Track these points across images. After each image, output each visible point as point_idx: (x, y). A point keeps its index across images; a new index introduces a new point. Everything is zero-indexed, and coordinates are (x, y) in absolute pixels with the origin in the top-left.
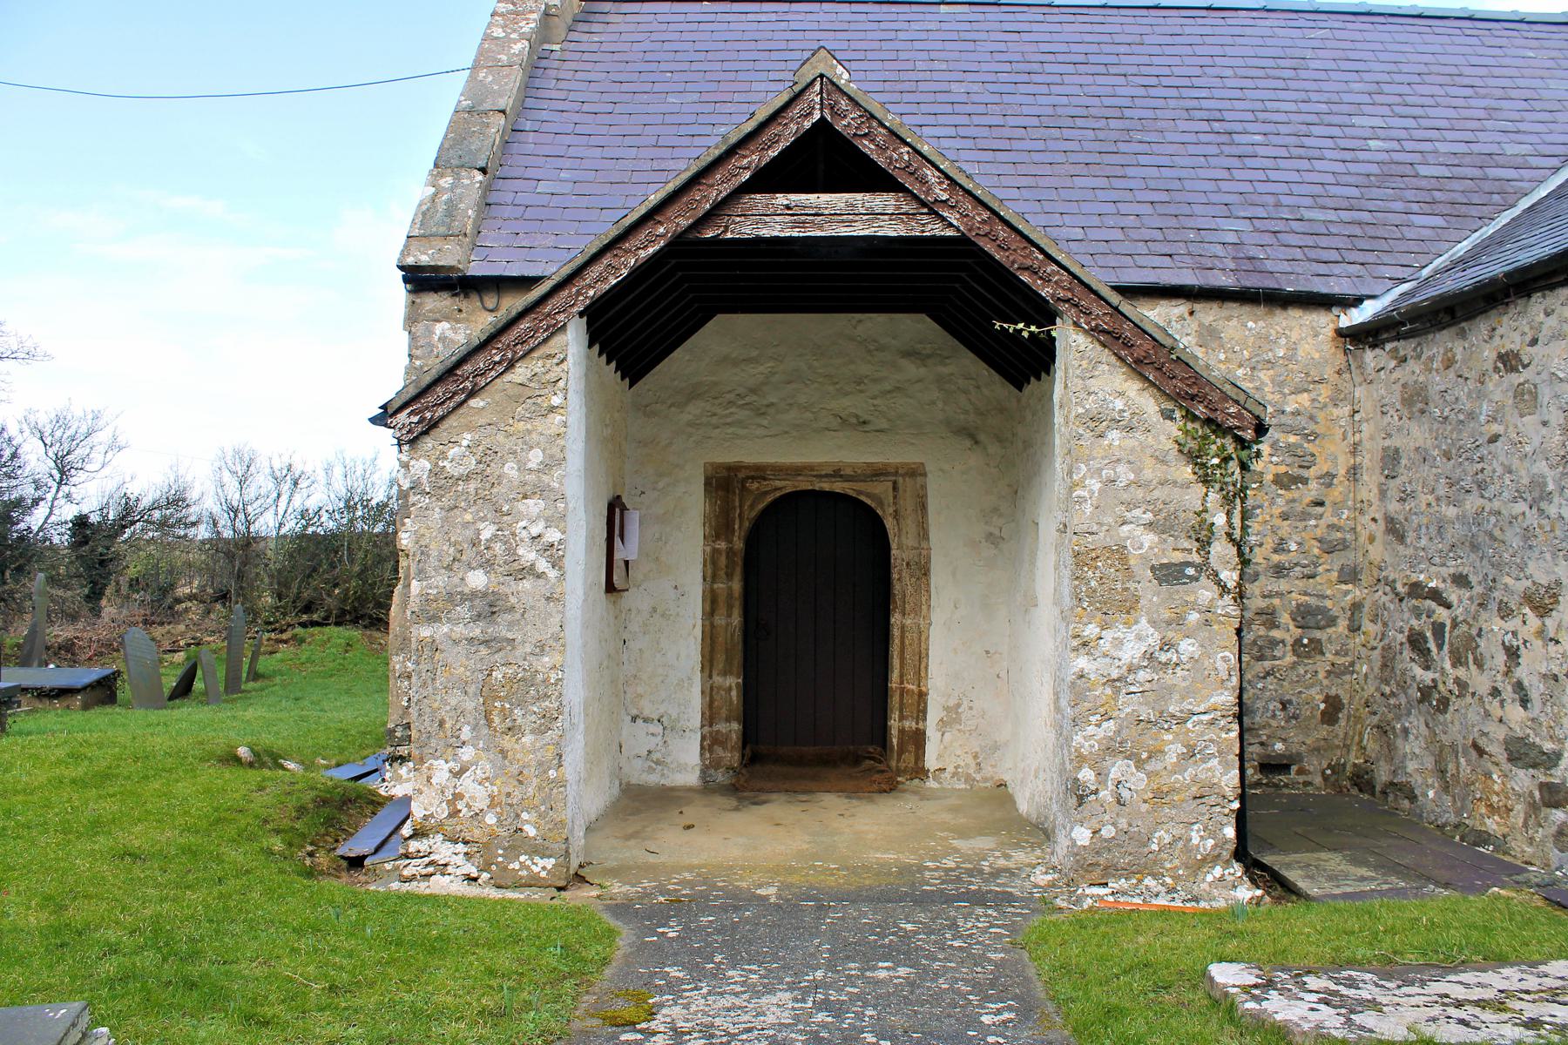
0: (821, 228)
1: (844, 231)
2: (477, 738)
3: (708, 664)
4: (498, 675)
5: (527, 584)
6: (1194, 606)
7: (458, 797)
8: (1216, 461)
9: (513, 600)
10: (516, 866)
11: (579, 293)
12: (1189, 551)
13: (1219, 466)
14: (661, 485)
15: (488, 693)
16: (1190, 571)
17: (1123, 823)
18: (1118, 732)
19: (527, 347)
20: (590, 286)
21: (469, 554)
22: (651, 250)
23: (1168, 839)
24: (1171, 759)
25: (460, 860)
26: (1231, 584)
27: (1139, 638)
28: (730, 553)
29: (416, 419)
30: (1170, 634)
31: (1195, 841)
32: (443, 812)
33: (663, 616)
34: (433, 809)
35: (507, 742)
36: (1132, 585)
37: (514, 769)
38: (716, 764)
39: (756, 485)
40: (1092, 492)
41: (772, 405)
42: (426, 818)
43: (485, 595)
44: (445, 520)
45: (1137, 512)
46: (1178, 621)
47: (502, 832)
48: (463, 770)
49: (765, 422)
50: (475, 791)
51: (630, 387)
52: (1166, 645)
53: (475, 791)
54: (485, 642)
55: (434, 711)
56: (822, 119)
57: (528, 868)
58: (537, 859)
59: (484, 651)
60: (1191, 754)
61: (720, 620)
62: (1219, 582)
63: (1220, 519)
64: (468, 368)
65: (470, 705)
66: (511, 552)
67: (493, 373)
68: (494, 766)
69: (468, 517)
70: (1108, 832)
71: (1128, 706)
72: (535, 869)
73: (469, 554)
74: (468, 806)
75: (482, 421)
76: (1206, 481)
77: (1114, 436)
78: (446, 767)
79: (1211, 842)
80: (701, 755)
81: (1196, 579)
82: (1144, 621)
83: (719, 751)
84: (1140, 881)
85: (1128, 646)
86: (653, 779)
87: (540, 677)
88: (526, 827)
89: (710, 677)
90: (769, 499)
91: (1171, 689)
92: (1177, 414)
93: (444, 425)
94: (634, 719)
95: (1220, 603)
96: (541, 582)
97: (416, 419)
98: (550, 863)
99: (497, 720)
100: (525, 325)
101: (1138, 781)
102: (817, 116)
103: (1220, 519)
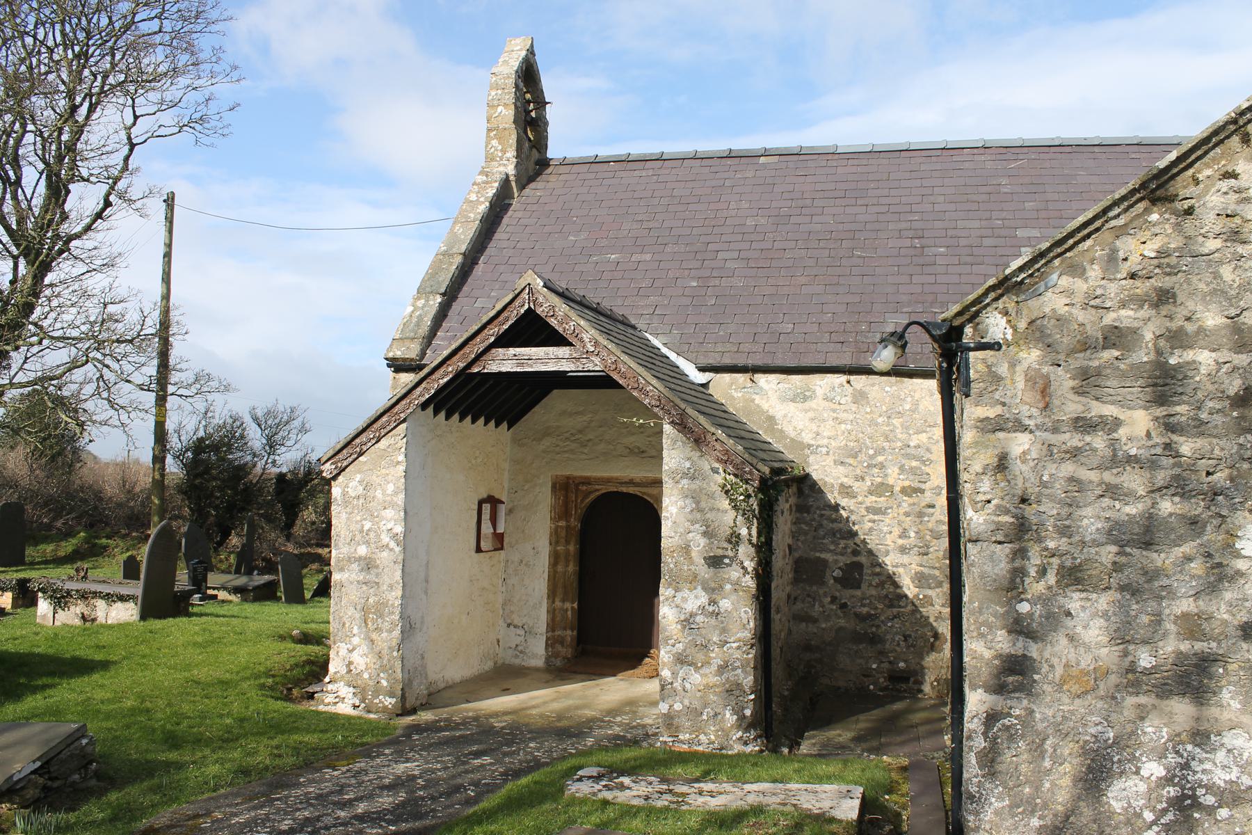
0: (532, 366)
2: (360, 633)
3: (552, 594)
4: (371, 600)
5: (385, 554)
6: (729, 581)
7: (350, 663)
8: (742, 497)
9: (378, 562)
10: (376, 701)
11: (410, 403)
12: (727, 549)
13: (744, 500)
14: (526, 488)
15: (365, 610)
16: (727, 561)
17: (686, 702)
19: (386, 431)
20: (415, 399)
21: (358, 537)
22: (445, 380)
26: (750, 569)
28: (568, 528)
29: (333, 467)
30: (714, 596)
32: (344, 670)
33: (526, 565)
34: (339, 669)
36: (693, 568)
38: (556, 655)
39: (585, 488)
40: (672, 514)
41: (589, 440)
42: (335, 673)
43: (365, 558)
44: (348, 519)
45: (697, 526)
47: (371, 683)
48: (354, 649)
49: (586, 451)
51: (509, 429)
55: (341, 618)
56: (530, 308)
59: (365, 588)
61: (560, 568)
62: (743, 568)
63: (744, 532)
64: (358, 441)
66: (378, 536)
67: (370, 444)
72: (386, 703)
73: (358, 537)
75: (366, 468)
76: (735, 508)
80: (546, 648)
81: (728, 565)
82: (699, 587)
83: (559, 647)
84: (697, 736)
85: (690, 602)
86: (517, 662)
88: (383, 681)
89: (553, 602)
90: (593, 497)
92: (721, 471)
93: (347, 470)
94: (509, 625)
95: (744, 579)
97: (333, 467)
98: (393, 701)
100: (384, 419)
102: (526, 307)
103: (744, 532)
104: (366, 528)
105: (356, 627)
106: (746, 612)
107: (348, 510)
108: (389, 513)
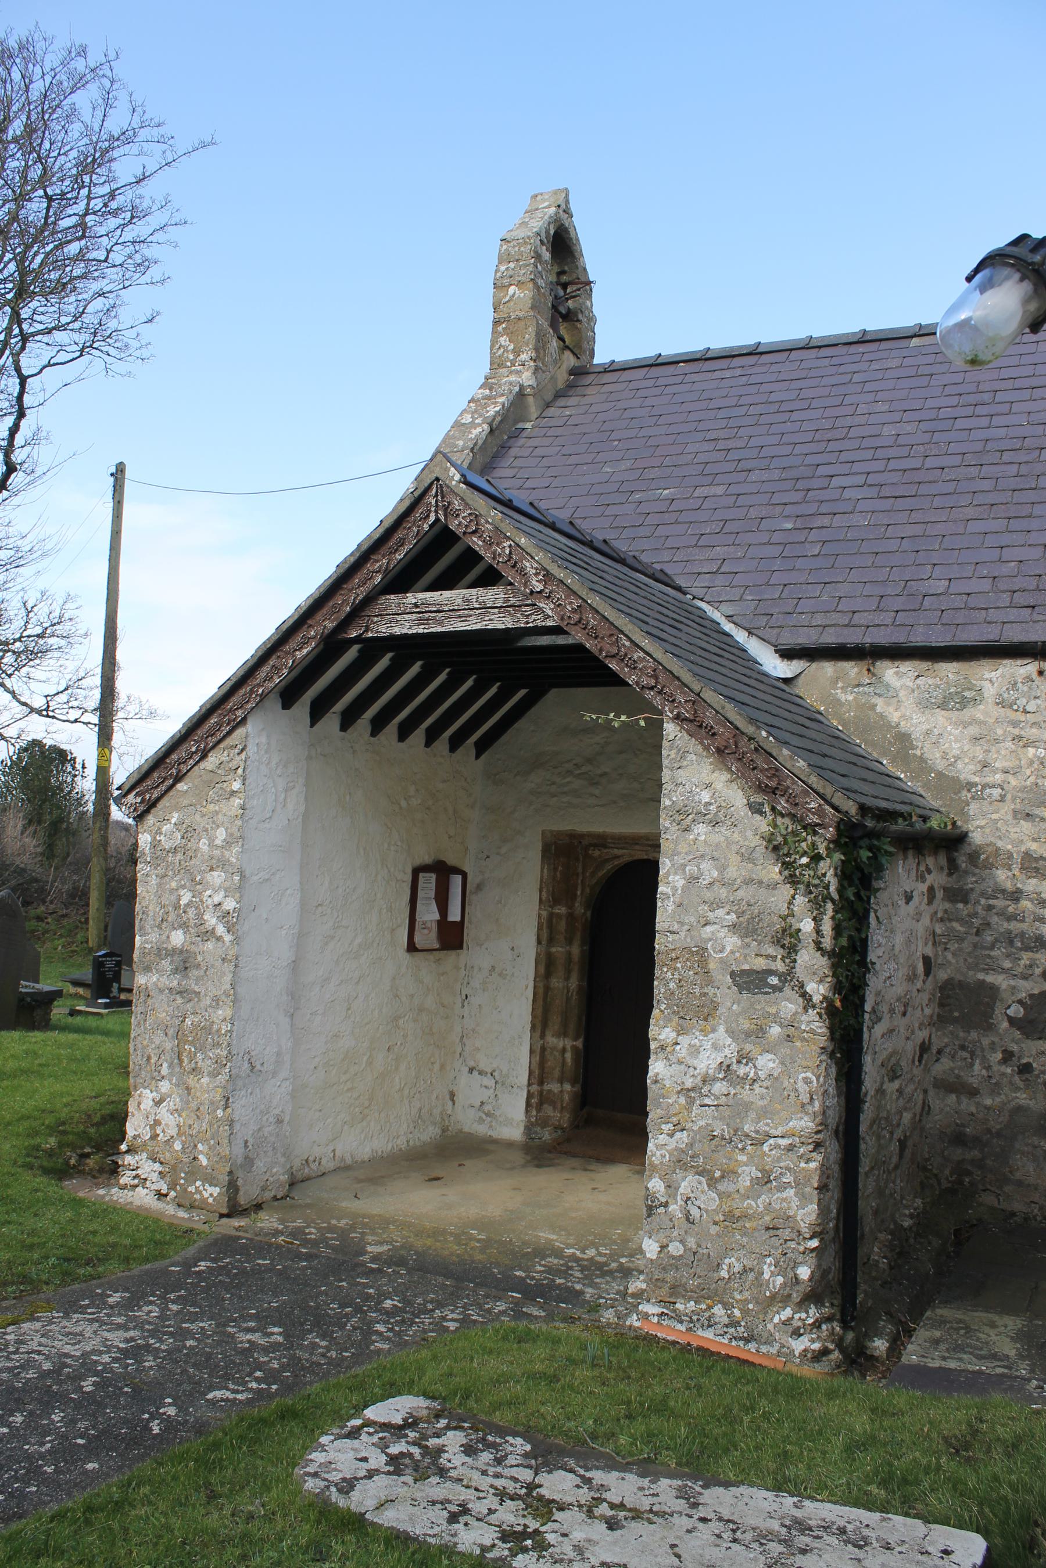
0: (441, 623)
1: (460, 626)
2: (171, 1074)
3: (541, 1022)
4: (188, 1022)
5: (210, 945)
6: (776, 1018)
7: (157, 1123)
8: (805, 860)
9: (200, 958)
11: (252, 692)
12: (774, 958)
13: (807, 865)
14: (503, 850)
16: (774, 980)
17: (691, 1243)
18: (690, 1145)
19: (215, 740)
20: (259, 685)
22: (305, 651)
23: (738, 1268)
24: (744, 1182)
25: (155, 1177)
26: (817, 999)
27: (715, 1047)
28: (571, 917)
29: (139, 800)
30: (748, 1047)
31: (766, 1276)
33: (500, 975)
35: (191, 1081)
36: (710, 991)
37: (194, 1105)
38: (543, 1123)
39: (597, 853)
40: (675, 889)
41: (605, 774)
42: (135, 1137)
43: (181, 952)
44: (159, 885)
45: (720, 913)
46: (760, 1032)
49: (597, 792)
50: (170, 1122)
51: (477, 757)
52: (744, 1058)
53: (170, 1122)
54: (179, 992)
55: (145, 1047)
56: (437, 520)
57: (200, 1193)
58: (207, 1186)
59: (179, 1000)
60: (765, 1180)
61: (556, 983)
62: (804, 995)
63: (807, 926)
64: (174, 757)
65: (168, 1045)
66: (200, 915)
67: (192, 762)
68: (181, 1100)
69: (174, 884)
70: (675, 1249)
71: (701, 1119)
72: (206, 1195)
74: (163, 1131)
75: (186, 802)
76: (793, 880)
77: (701, 830)
78: (151, 1096)
79: (780, 1280)
80: (527, 1111)
81: (776, 989)
82: (722, 1029)
83: (548, 1110)
84: (710, 1307)
85: (704, 1055)
86: (481, 1130)
87: (215, 1027)
88: (201, 1157)
89: (543, 1036)
90: (609, 867)
91: (747, 1106)
92: (767, 809)
93: (160, 805)
94: (471, 1070)
95: (804, 1018)
96: (220, 944)
98: (216, 1191)
99: (186, 1060)
100: (213, 720)
101: (709, 1200)
102: (432, 518)
103: (807, 926)
104: (184, 901)
105: (165, 1065)
106: (807, 1081)
107: (160, 871)
108: (217, 877)
